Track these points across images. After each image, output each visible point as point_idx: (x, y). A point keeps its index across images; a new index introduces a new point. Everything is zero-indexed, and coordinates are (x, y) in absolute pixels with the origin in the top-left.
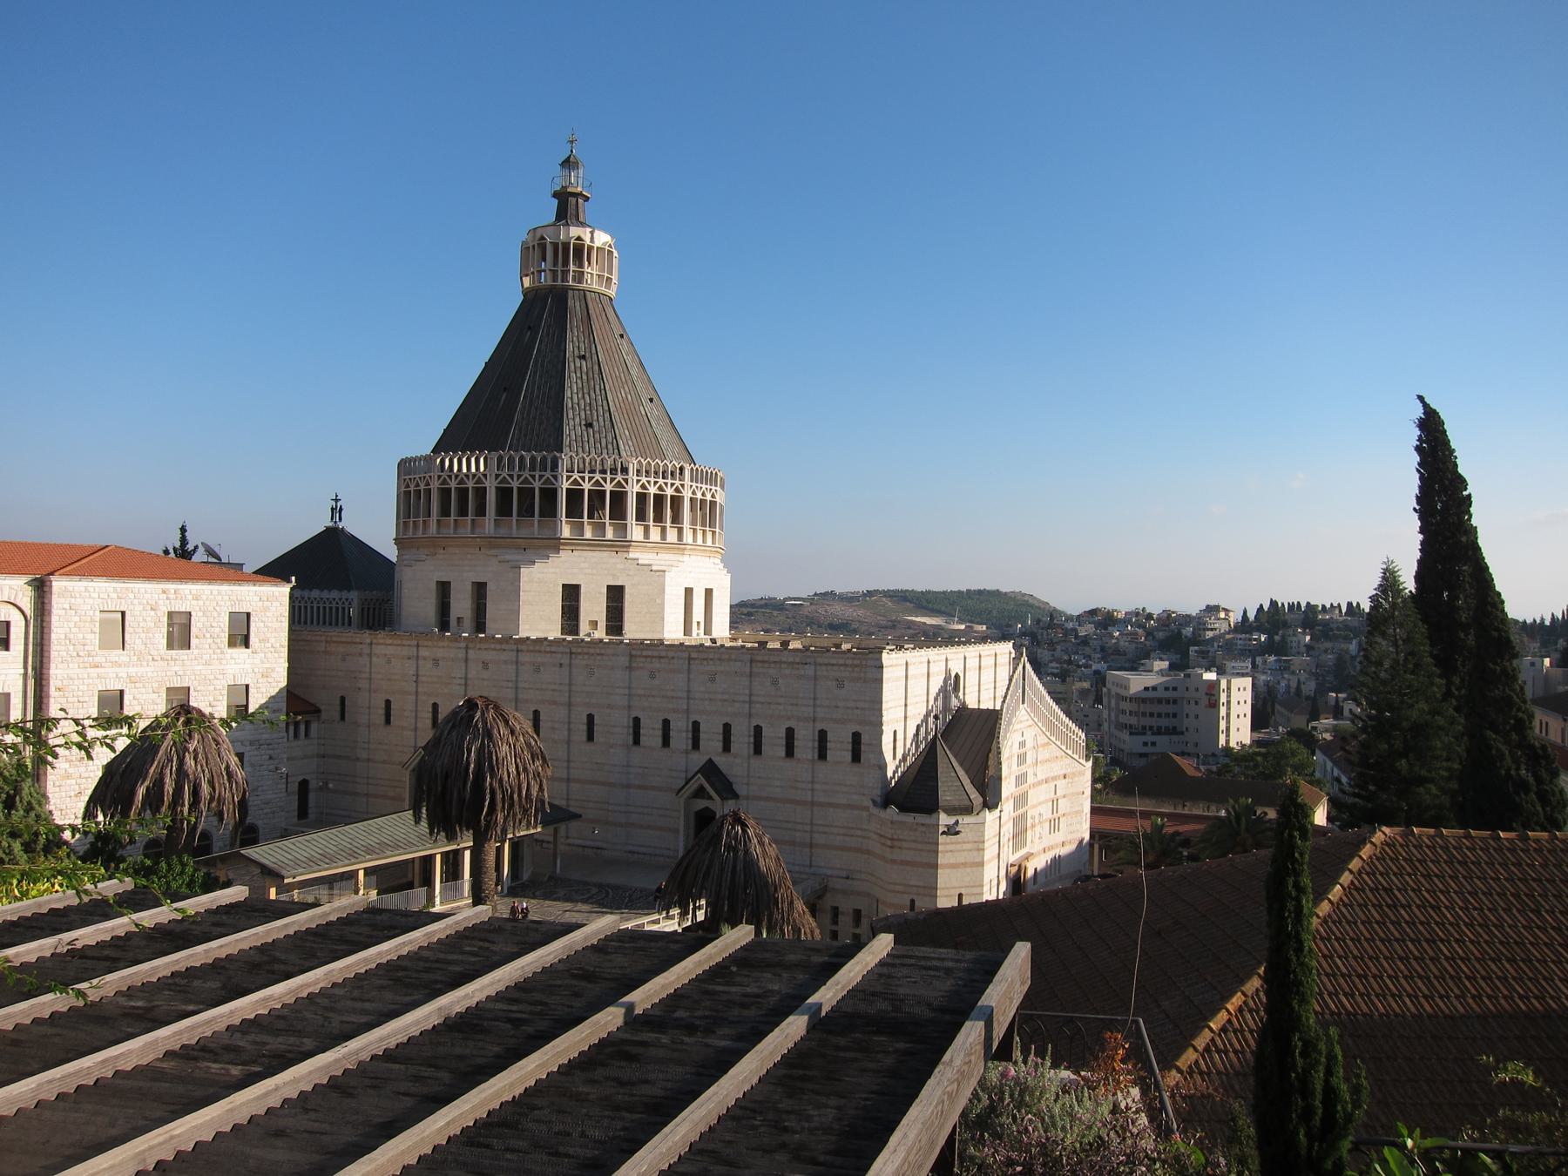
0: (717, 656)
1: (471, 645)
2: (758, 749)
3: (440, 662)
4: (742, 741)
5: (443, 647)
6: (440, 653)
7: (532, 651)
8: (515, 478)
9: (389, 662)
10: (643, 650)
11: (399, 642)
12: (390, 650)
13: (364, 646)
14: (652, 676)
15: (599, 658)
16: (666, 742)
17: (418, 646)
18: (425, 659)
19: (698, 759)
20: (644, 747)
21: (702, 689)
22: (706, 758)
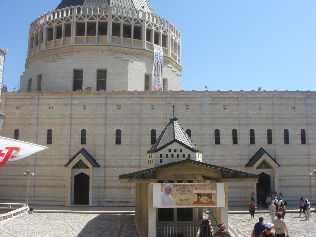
0: (262, 96)
1: (108, 96)
2: (287, 141)
3: (87, 107)
4: (278, 138)
5: (89, 98)
6: (86, 101)
7: (150, 98)
8: (122, 18)
9: (51, 108)
10: (219, 94)
11: (59, 97)
12: (51, 102)
13: (34, 100)
14: (225, 108)
15: (193, 99)
16: (235, 141)
17: (72, 98)
18: (76, 105)
19: (254, 149)
20: (223, 145)
21: (255, 113)
22: (259, 148)
